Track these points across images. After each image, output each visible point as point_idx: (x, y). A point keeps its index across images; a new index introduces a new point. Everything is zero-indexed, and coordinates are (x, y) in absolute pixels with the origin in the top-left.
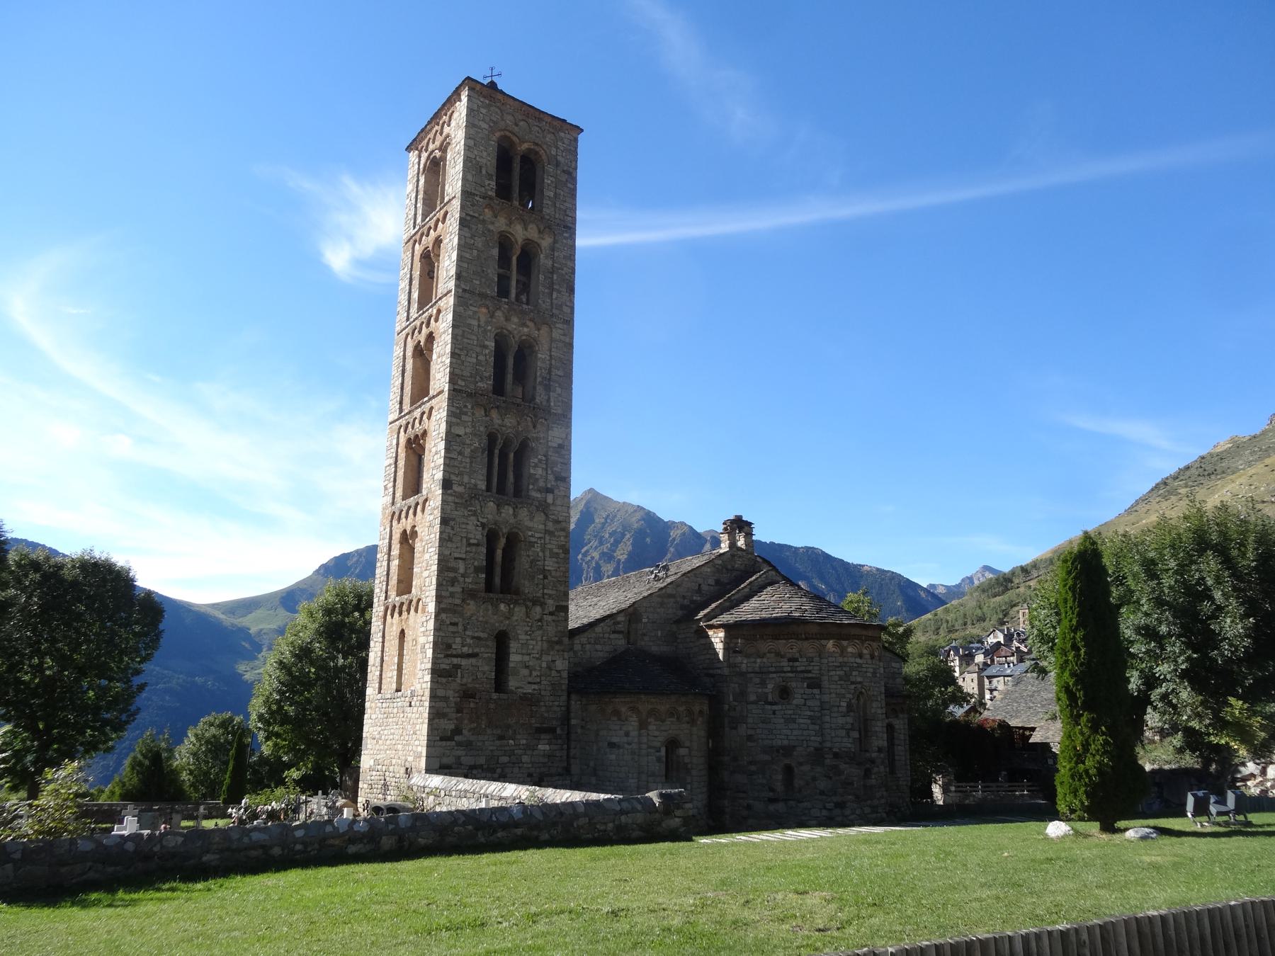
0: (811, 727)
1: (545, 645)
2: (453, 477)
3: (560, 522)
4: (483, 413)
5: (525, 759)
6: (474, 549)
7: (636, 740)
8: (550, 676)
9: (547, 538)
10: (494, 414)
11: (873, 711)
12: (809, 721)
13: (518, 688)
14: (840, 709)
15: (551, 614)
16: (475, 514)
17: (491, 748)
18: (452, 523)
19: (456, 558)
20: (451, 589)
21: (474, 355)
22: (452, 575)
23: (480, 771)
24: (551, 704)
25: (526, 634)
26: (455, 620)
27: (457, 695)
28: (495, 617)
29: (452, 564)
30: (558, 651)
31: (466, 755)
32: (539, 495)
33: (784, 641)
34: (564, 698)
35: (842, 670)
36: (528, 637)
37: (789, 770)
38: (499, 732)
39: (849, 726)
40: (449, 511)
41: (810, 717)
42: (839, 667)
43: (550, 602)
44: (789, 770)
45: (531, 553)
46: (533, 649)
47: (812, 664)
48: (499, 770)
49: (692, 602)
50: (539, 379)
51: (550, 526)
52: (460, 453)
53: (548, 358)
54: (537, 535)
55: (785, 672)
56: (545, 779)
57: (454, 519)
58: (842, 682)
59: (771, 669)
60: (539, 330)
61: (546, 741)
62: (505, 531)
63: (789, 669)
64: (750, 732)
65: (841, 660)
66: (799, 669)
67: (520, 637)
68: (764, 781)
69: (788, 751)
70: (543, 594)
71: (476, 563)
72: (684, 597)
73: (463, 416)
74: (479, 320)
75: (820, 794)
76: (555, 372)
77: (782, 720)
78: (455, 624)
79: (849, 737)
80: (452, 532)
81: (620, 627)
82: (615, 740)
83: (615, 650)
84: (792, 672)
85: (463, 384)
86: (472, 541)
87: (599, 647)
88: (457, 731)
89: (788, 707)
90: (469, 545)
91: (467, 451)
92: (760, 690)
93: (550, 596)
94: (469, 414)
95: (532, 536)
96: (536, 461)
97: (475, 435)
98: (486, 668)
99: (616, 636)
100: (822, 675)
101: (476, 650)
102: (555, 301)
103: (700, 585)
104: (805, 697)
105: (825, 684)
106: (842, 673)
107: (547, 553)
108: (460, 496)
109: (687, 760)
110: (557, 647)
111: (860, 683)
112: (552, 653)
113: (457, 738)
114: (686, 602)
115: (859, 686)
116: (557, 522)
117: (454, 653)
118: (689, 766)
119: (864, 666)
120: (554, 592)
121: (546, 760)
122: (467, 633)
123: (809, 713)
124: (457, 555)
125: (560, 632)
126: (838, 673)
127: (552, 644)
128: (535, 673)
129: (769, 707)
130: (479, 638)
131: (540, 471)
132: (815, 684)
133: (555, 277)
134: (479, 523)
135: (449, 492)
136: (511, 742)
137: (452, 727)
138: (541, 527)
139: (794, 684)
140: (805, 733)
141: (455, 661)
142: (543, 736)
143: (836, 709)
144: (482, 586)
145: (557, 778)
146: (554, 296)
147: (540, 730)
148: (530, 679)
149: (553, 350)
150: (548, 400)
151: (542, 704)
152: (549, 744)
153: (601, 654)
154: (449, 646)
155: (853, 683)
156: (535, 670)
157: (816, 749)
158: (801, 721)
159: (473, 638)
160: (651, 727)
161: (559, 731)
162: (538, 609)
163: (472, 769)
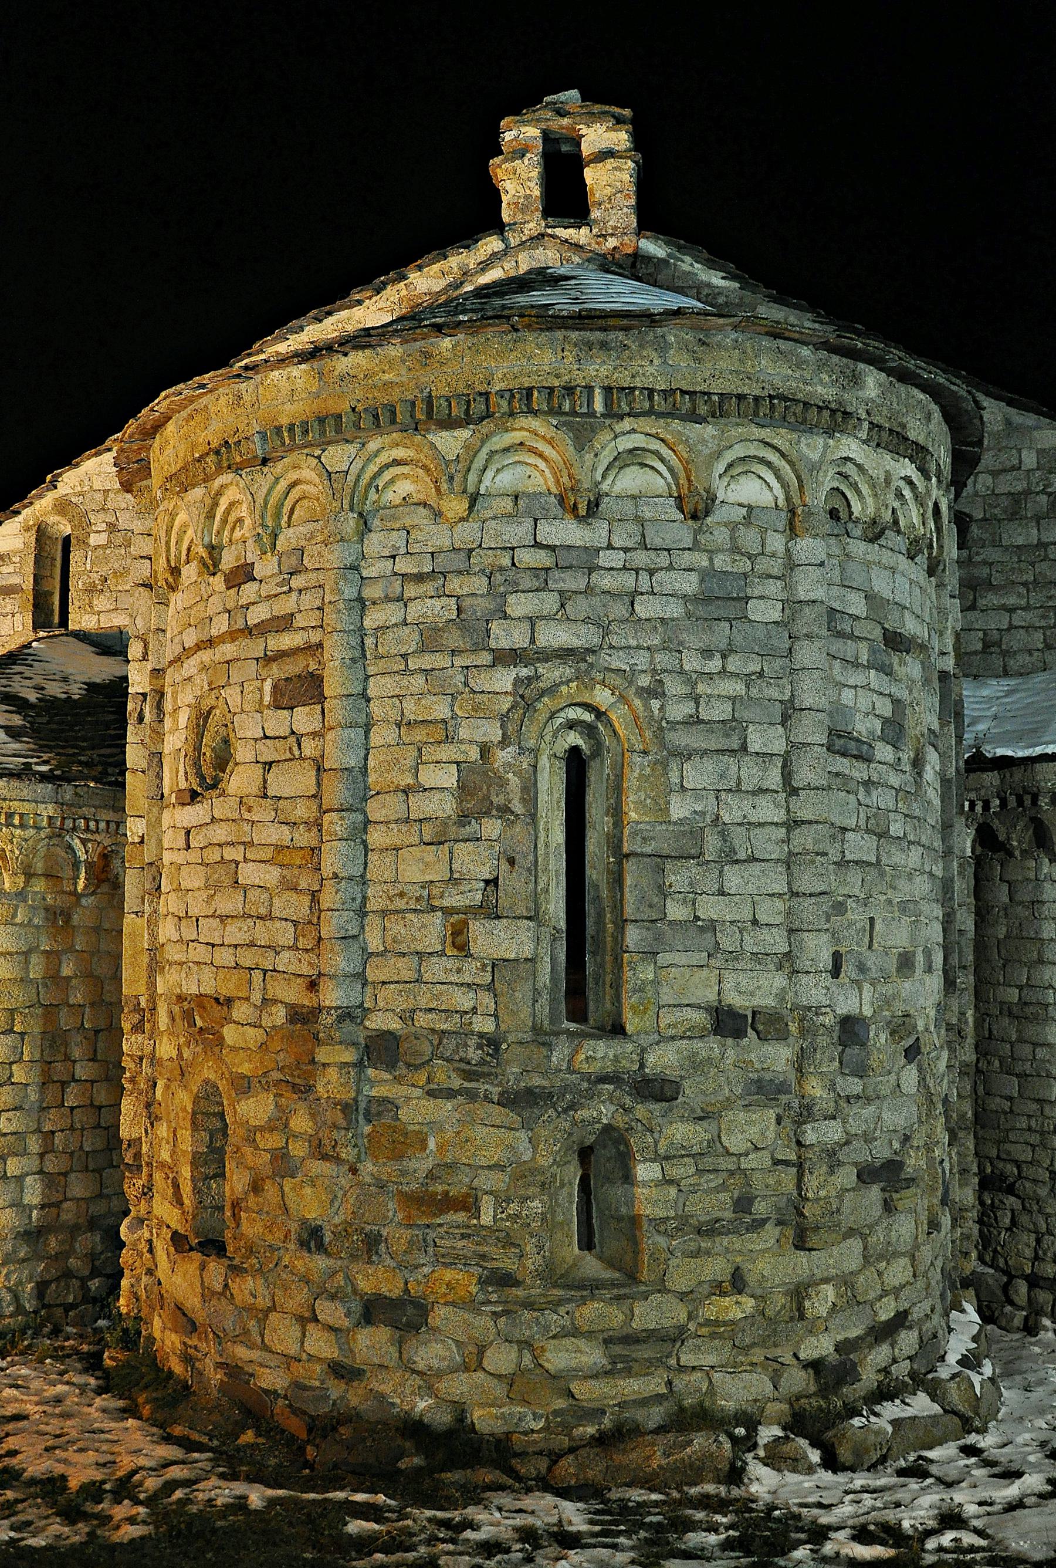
11: (679, 809)
12: (271, 875)
42: (420, 578)
47: (297, 582)
66: (257, 615)
75: (303, 1244)
84: (232, 635)
111: (566, 654)
115: (551, 673)
119: (606, 559)
123: (281, 834)
140: (262, 933)
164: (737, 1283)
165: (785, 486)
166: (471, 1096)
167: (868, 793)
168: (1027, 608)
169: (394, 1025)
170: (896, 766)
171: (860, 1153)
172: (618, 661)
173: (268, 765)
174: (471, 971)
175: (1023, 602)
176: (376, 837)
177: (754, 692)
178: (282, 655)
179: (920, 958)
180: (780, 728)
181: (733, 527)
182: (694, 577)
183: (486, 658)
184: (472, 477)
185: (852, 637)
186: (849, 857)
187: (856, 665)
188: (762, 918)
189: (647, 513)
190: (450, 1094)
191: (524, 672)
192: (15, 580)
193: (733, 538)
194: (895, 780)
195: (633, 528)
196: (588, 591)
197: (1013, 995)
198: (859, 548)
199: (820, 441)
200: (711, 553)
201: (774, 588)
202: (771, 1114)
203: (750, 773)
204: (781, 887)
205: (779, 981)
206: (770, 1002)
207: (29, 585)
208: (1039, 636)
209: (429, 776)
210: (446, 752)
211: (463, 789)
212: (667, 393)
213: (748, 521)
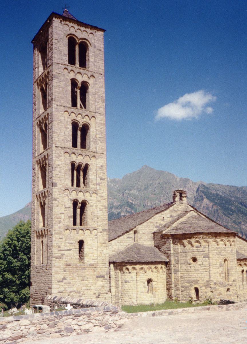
0: (205, 273)
1: (99, 245)
2: (58, 182)
3: (103, 196)
4: (68, 155)
5: (92, 288)
6: (67, 209)
7: (135, 279)
9: (98, 203)
10: (73, 155)
11: (231, 266)
12: (204, 271)
13: (88, 261)
14: (217, 265)
15: (101, 232)
16: (67, 196)
17: (78, 284)
18: (58, 200)
19: (60, 213)
20: (59, 225)
21: (63, 132)
23: (74, 293)
24: (102, 266)
26: (61, 237)
27: (64, 265)
28: (78, 235)
29: (59, 215)
30: (104, 246)
31: (69, 287)
32: (93, 186)
33: (194, 240)
34: (108, 264)
35: (218, 250)
37: (197, 290)
38: (81, 278)
39: (221, 272)
40: (56, 195)
41: (204, 269)
42: (216, 249)
43: (100, 228)
44: (197, 290)
46: (94, 246)
47: (205, 248)
48: (82, 292)
49: (160, 225)
50: (91, 140)
51: (99, 199)
52: (60, 172)
53: (95, 130)
54: (93, 202)
55: (194, 252)
56: (101, 295)
57: (59, 198)
58: (218, 255)
59: (190, 251)
60: (90, 119)
61: (101, 281)
62: (80, 201)
63: (196, 250)
64: (182, 275)
65: (217, 246)
67: (88, 242)
68: (187, 294)
69: (196, 282)
70: (97, 225)
71: (69, 215)
72: (157, 223)
73: (60, 157)
74: (64, 117)
76: (97, 136)
77: (194, 270)
79: (220, 276)
80: (58, 203)
81: (131, 236)
82: (127, 279)
83: (129, 245)
84: (197, 252)
85: (59, 144)
86: (67, 206)
87: (122, 244)
88: (65, 279)
89: (196, 265)
90: (66, 208)
91: (63, 171)
92: (185, 259)
93: (100, 226)
94: (63, 156)
95: (91, 203)
96: (92, 173)
97: (66, 164)
98: (75, 254)
99: (129, 239)
100: (209, 252)
101: (71, 248)
102: (96, 107)
103: (163, 218)
104: (203, 261)
105: (211, 256)
106: (217, 252)
107: (98, 209)
108: (61, 189)
109: (155, 286)
110: (104, 245)
111: (225, 255)
112: (102, 247)
113: (64, 281)
114: (158, 225)
115: (225, 256)
116: (102, 196)
117: (62, 249)
118: (157, 289)
120: (101, 224)
121: (101, 288)
122: (66, 241)
123: (204, 267)
124: (60, 212)
125: (105, 239)
126: (216, 251)
129: (189, 265)
130: (72, 243)
132: (207, 256)
133: (96, 96)
134: (69, 199)
135: (56, 187)
136: (86, 282)
137: (62, 277)
138: (96, 199)
139: (197, 257)
141: (62, 252)
142: (99, 279)
143: (215, 265)
145: (106, 294)
146: (96, 104)
147: (97, 277)
148: (93, 258)
149: (97, 127)
150: (96, 148)
151: (98, 267)
152: (102, 282)
153: (123, 246)
154: (59, 247)
155: (222, 255)
157: (207, 281)
158: (201, 270)
159: (69, 243)
160: (141, 274)
161: (106, 277)
162: (95, 231)
163: (71, 292)
169: (216, 281)
172: (228, 255)
173: (203, 262)
174: (221, 277)
178: (204, 254)
190: (220, 286)
192: (131, 237)
207: (133, 237)
209: (217, 263)
210: (219, 262)
211: (220, 264)
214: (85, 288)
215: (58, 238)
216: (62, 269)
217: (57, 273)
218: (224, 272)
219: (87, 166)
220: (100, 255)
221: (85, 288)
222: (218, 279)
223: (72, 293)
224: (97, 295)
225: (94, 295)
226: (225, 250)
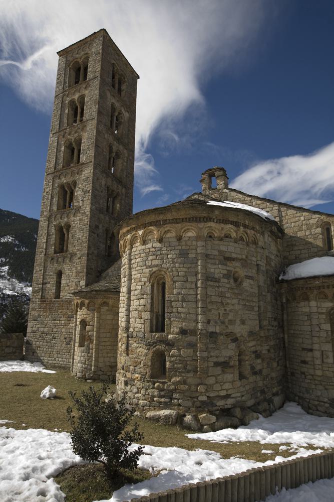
5: (63, 330)
8: (76, 289)
14: (137, 292)
15: (79, 259)
22: (41, 250)
25: (69, 270)
32: (78, 204)
35: (140, 257)
36: (69, 271)
45: (73, 231)
54: (76, 222)
78: (41, 271)
88: (39, 316)
93: (78, 250)
95: (74, 223)
110: (81, 274)
111: (157, 266)
116: (84, 213)
127: (77, 273)
128: (71, 289)
131: (79, 193)
136: (58, 322)
137: (37, 314)
144: (53, 252)
148: (69, 291)
156: (72, 287)
164: (185, 383)
165: (196, 232)
166: (141, 343)
167: (218, 288)
168: (304, 249)
170: (228, 283)
171: (215, 360)
175: (303, 248)
176: (132, 298)
177: (189, 270)
179: (238, 322)
180: (195, 277)
181: (186, 241)
182: (178, 251)
183: (145, 267)
184: (144, 238)
185: (214, 259)
186: (212, 301)
187: (215, 264)
188: (191, 312)
189: (170, 240)
191: (150, 269)
193: (186, 243)
194: (228, 286)
195: (168, 243)
196: (161, 254)
197: (292, 332)
198: (217, 242)
199: (203, 224)
200: (182, 246)
201: (194, 251)
202: (192, 350)
203: (188, 285)
204: (194, 307)
205: (194, 324)
206: (192, 328)
208: (307, 255)
210: (140, 283)
212: (173, 220)
213: (189, 240)
214: (55, 330)
215: (38, 270)
216: (38, 305)
217: (34, 310)
218: (148, 307)
219: (75, 183)
220: (76, 287)
221: (55, 330)
222: (136, 325)
223: (43, 335)
224: (67, 340)
225: (64, 340)
226: (159, 253)
